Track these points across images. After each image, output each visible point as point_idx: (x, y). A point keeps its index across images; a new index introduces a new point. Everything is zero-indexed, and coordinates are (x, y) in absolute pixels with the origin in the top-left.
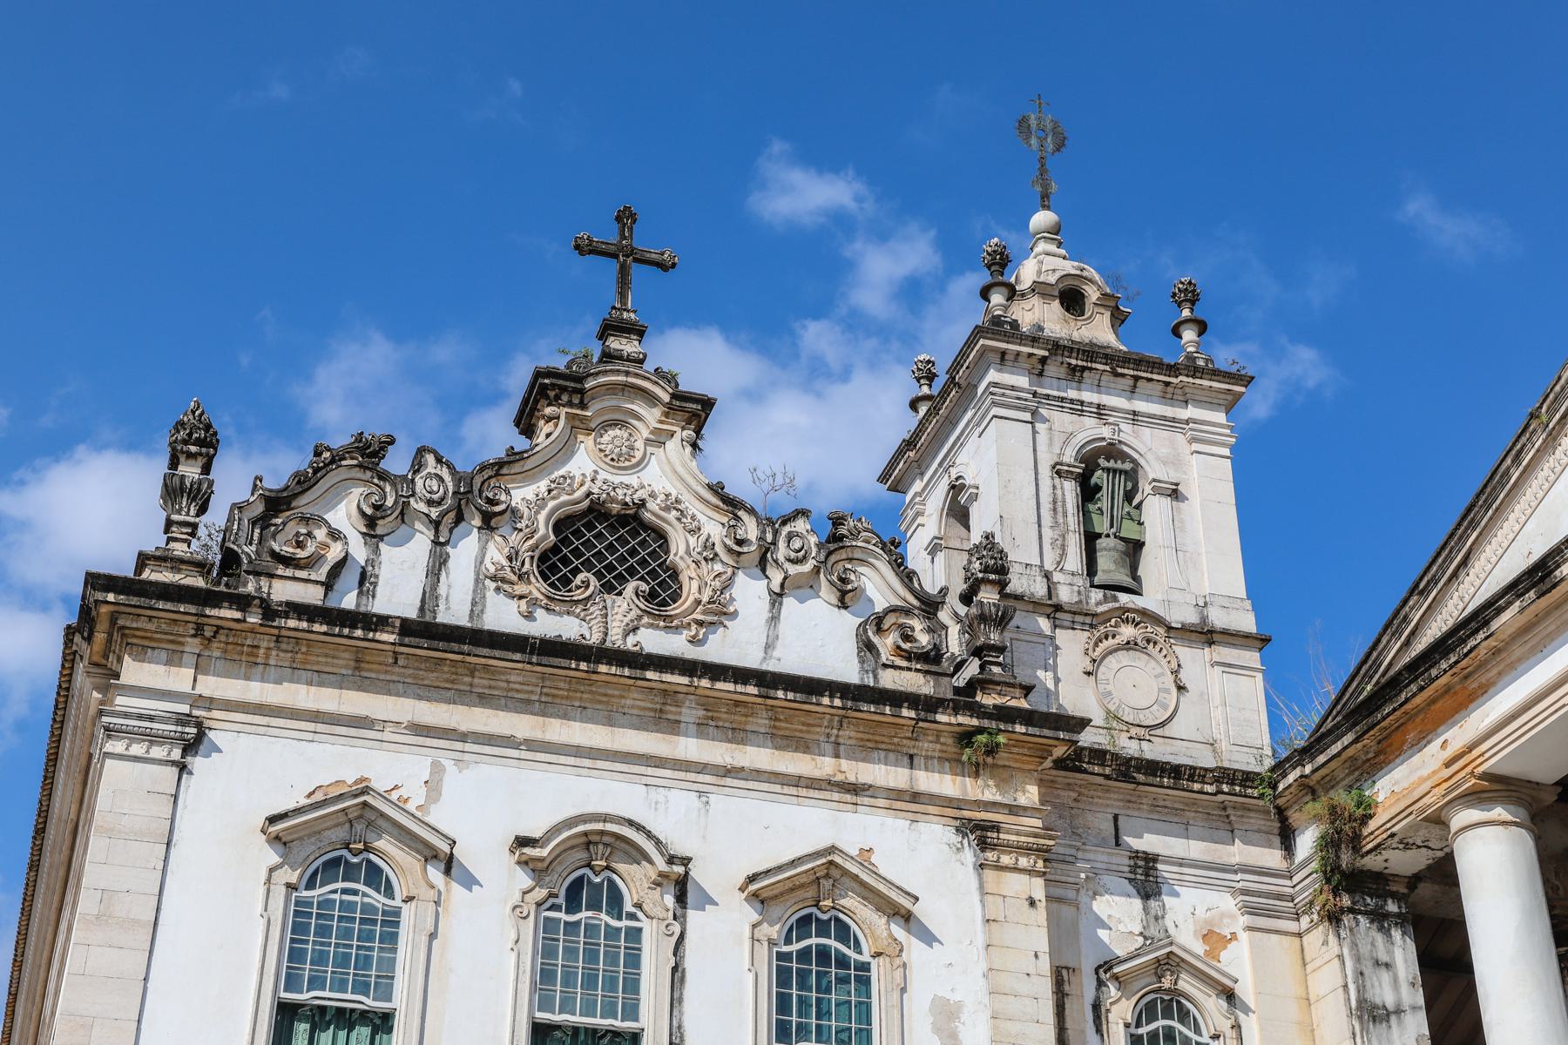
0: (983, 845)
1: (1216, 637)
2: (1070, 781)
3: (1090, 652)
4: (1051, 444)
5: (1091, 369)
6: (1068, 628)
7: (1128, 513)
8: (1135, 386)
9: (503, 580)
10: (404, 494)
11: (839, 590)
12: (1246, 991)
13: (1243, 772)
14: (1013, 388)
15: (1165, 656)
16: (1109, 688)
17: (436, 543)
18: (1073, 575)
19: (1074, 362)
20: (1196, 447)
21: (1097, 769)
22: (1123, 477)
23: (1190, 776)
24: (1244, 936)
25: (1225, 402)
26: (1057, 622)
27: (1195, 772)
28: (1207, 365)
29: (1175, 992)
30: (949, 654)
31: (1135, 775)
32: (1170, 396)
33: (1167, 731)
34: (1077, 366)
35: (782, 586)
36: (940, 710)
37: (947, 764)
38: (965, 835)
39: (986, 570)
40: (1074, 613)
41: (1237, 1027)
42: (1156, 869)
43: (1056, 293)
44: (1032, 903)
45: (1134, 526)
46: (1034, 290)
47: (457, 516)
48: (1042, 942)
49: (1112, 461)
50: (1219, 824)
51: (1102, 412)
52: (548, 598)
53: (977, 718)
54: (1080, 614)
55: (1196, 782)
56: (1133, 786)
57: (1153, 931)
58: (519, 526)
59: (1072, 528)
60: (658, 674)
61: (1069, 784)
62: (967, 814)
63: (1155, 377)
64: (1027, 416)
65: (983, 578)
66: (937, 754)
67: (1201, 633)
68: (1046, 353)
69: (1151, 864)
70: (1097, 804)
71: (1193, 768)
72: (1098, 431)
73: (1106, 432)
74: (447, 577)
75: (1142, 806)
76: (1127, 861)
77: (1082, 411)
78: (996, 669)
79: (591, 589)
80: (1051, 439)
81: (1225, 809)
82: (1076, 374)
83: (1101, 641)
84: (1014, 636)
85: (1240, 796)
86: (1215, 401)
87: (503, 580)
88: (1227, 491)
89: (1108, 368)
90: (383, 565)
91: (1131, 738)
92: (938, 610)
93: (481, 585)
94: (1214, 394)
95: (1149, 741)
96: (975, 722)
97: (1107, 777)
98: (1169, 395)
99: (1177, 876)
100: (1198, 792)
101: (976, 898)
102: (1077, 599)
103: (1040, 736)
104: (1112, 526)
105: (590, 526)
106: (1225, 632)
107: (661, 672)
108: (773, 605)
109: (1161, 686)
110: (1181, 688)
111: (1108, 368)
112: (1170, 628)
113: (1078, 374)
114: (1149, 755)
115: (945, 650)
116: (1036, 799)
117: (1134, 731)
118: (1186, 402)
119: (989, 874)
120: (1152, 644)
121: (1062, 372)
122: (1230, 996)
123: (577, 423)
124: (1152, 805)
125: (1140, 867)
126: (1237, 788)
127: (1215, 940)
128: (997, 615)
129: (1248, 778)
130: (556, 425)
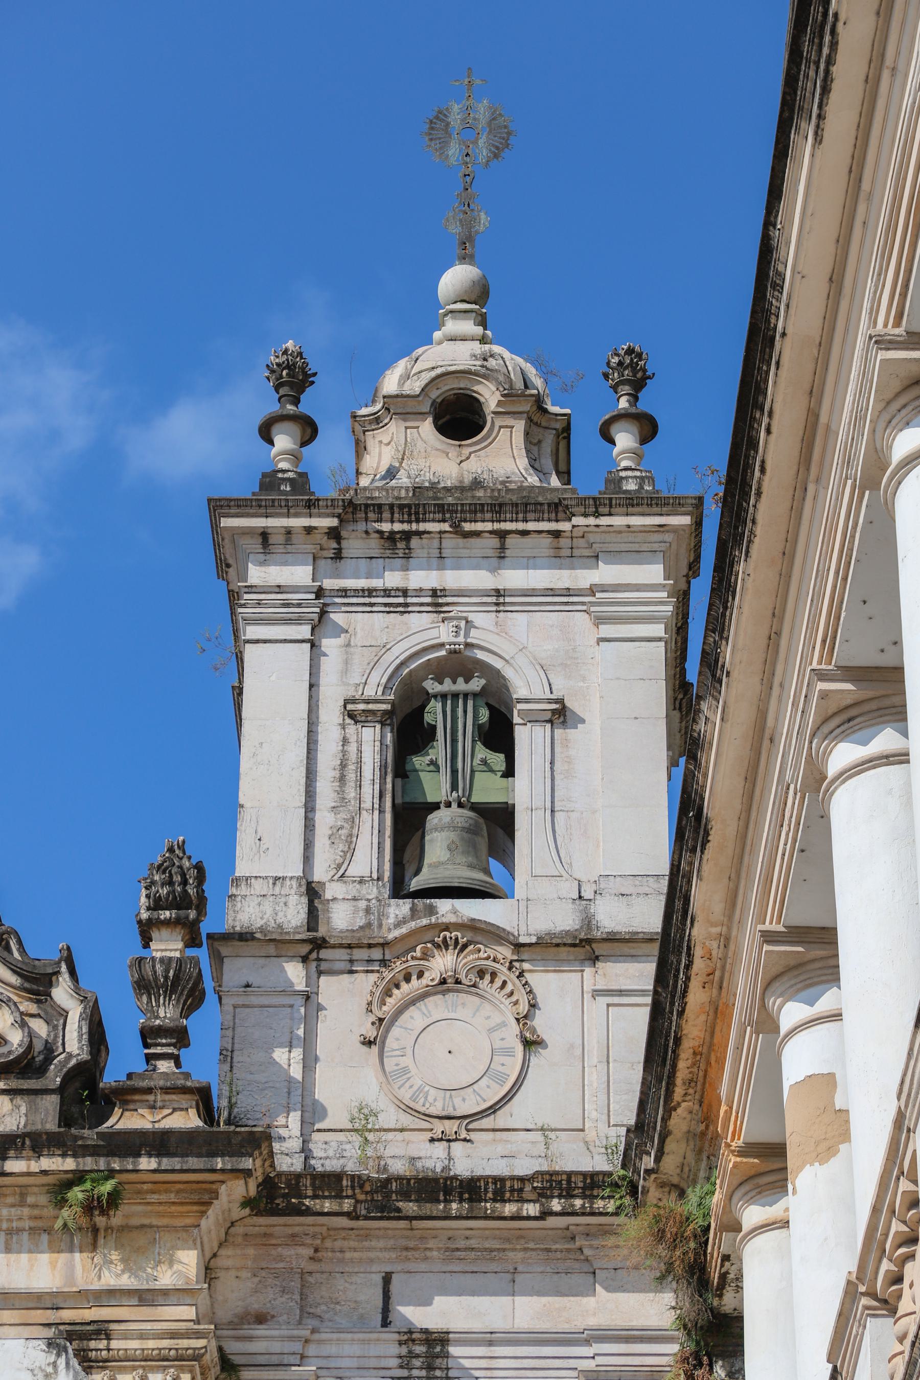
1: (599, 949)
2: (297, 1229)
3: (374, 1008)
5: (419, 534)
6: (342, 972)
7: (484, 762)
8: (503, 548)
13: (584, 1175)
14: (280, 589)
15: (511, 994)
16: (407, 1061)
18: (360, 882)
19: (386, 527)
20: (607, 630)
21: (327, 1206)
22: (470, 703)
23: (495, 1193)
25: (663, 547)
26: (324, 966)
27: (503, 1186)
28: (641, 487)
30: (63, 1056)
31: (400, 1204)
32: (567, 552)
33: (501, 1119)
34: (392, 533)
36: (12, 1153)
37: (45, 1237)
39: (157, 904)
40: (349, 946)
42: (447, 1356)
43: (426, 408)
45: (497, 781)
46: (388, 410)
49: (447, 681)
50: (569, 1263)
51: (440, 600)
53: (74, 1156)
54: (359, 946)
55: (510, 1201)
56: (402, 1224)
59: (367, 804)
61: (293, 1236)
63: (531, 526)
64: (304, 631)
65: (149, 920)
66: (27, 1224)
67: (574, 945)
68: (334, 522)
69: (438, 1349)
70: (352, 1260)
71: (499, 1180)
72: (434, 633)
73: (445, 633)
75: (428, 1254)
76: (395, 1350)
77: (406, 605)
78: (164, 1066)
80: (346, 662)
81: (573, 1238)
83: (397, 986)
84: (240, 1001)
85: (583, 1214)
86: (645, 547)
89: (446, 527)
91: (432, 1140)
92: (50, 985)
94: (640, 537)
95: (465, 1140)
96: (70, 1164)
97: (348, 1215)
99: (483, 1363)
100: (513, 1218)
102: (361, 921)
103: (182, 1171)
104: (454, 787)
106: (612, 939)
109: (498, 1044)
110: (531, 1044)
111: (448, 529)
112: (518, 947)
113: (401, 545)
115: (61, 1050)
117: (439, 1127)
118: (597, 557)
120: (488, 977)
121: (374, 545)
124: (447, 1249)
125: (418, 1356)
126: (578, 1203)
128: (166, 978)
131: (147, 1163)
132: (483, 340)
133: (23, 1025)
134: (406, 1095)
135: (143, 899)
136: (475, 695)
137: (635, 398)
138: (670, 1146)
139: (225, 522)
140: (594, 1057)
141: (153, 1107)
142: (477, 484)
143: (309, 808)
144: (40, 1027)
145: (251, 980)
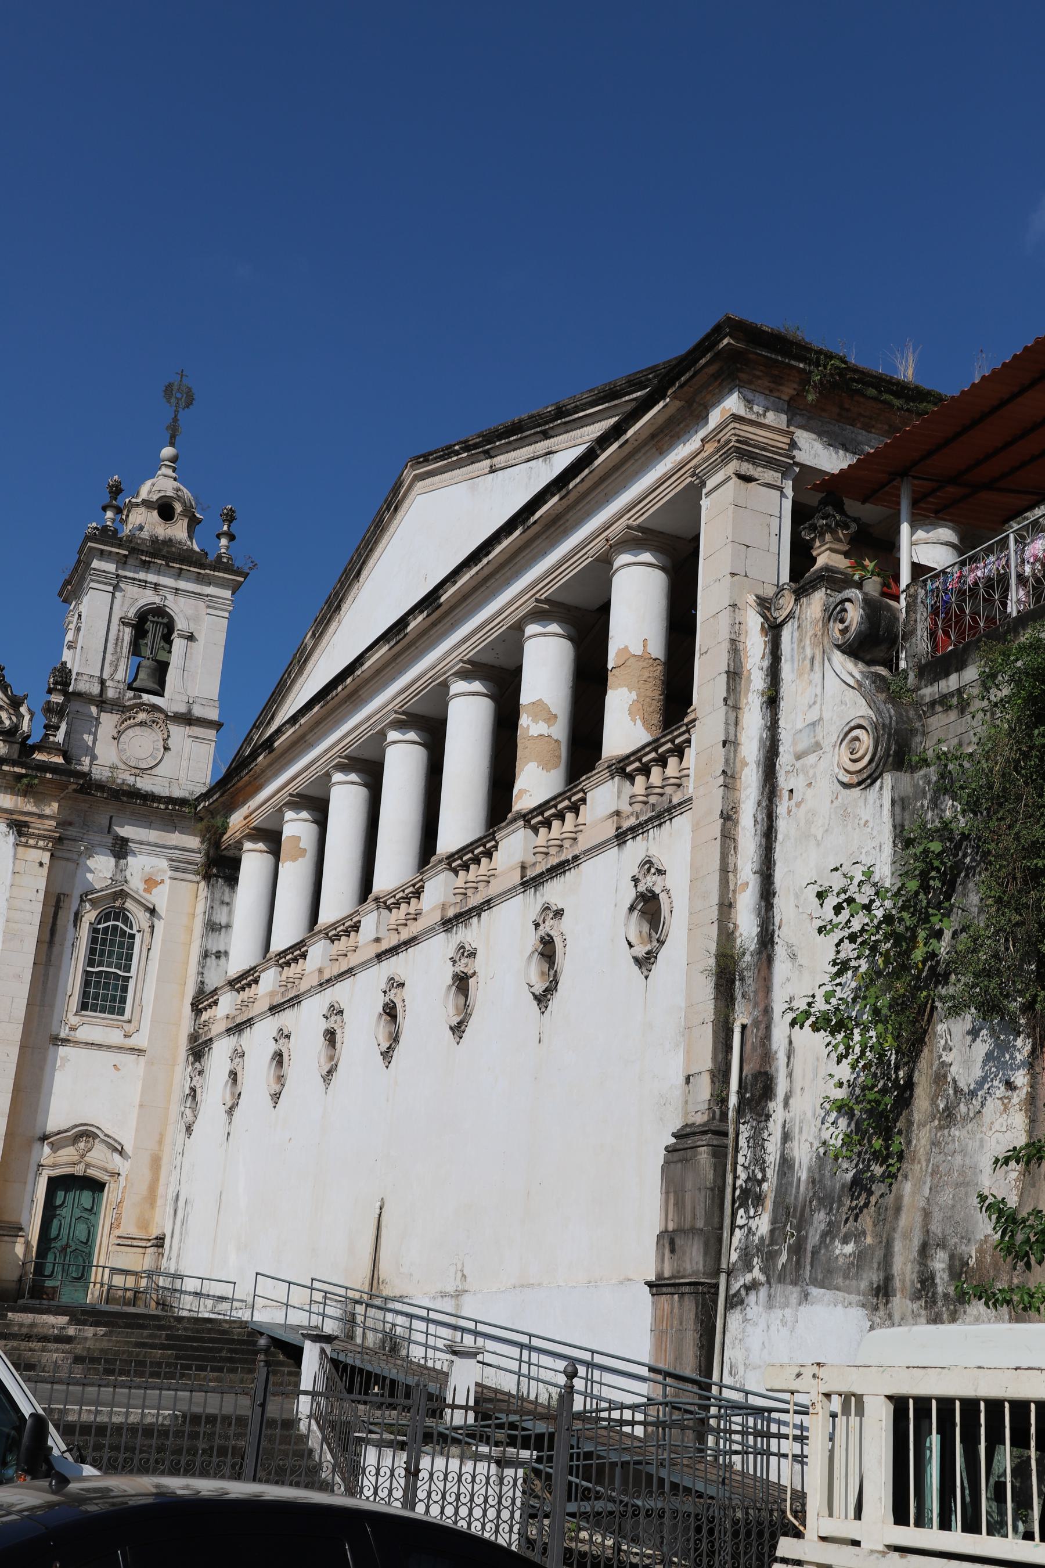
0: (20, 834)
4: (122, 605)
12: (161, 909)
14: (104, 572)
19: (144, 558)
20: (210, 611)
24: (168, 881)
29: (123, 909)
33: (153, 772)
38: (11, 828)
39: (56, 683)
41: (152, 927)
44: (41, 864)
45: (165, 654)
48: (42, 885)
57: (118, 877)
62: (15, 817)
63: (192, 569)
64: (111, 589)
68: (126, 553)
73: (157, 600)
76: (111, 841)
82: (146, 566)
88: (221, 638)
96: (23, 771)
98: (200, 579)
101: (11, 860)
102: (117, 696)
110: (166, 749)
112: (167, 716)
114: (139, 785)
116: (56, 810)
117: (134, 771)
119: (20, 849)
121: (137, 563)
122: (152, 911)
127: (151, 883)
129: (182, 802)
131: (49, 776)
132: (175, 479)
133: (11, 719)
134: (124, 758)
135: (52, 680)
136: (164, 624)
137: (229, 527)
138: (216, 804)
139: (89, 544)
140: (186, 756)
141: (49, 753)
142: (169, 542)
143: (105, 652)
144: (14, 719)
145: (80, 710)
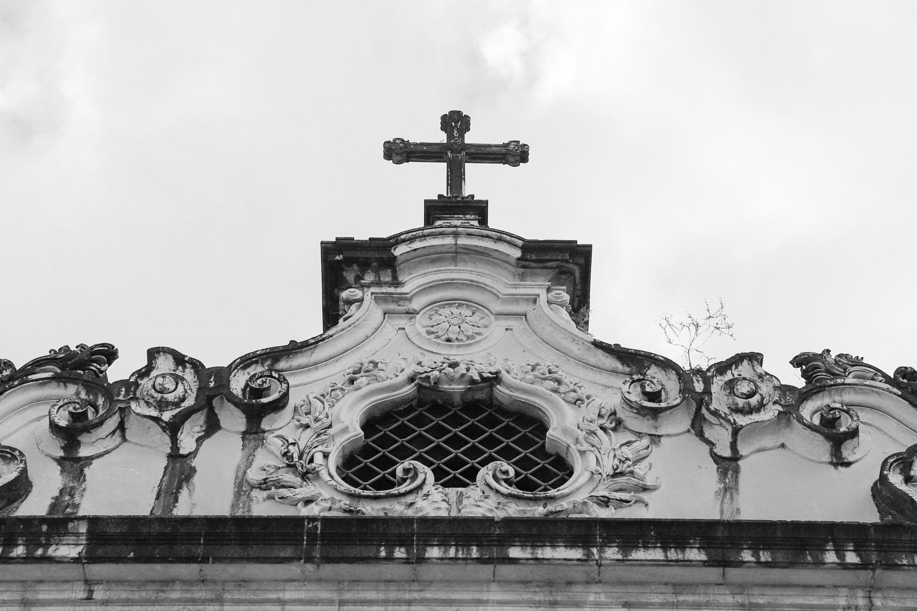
9: (280, 485)
10: (121, 398)
11: (828, 437)
17: (174, 456)
35: (733, 446)
47: (207, 422)
52: (351, 495)
58: (305, 420)
60: (529, 550)
74: (190, 494)
79: (421, 477)
87: (280, 485)
90: (86, 494)
93: (244, 498)
105: (420, 421)
107: (534, 546)
108: (723, 473)
123: (392, 307)
130: (359, 307)
